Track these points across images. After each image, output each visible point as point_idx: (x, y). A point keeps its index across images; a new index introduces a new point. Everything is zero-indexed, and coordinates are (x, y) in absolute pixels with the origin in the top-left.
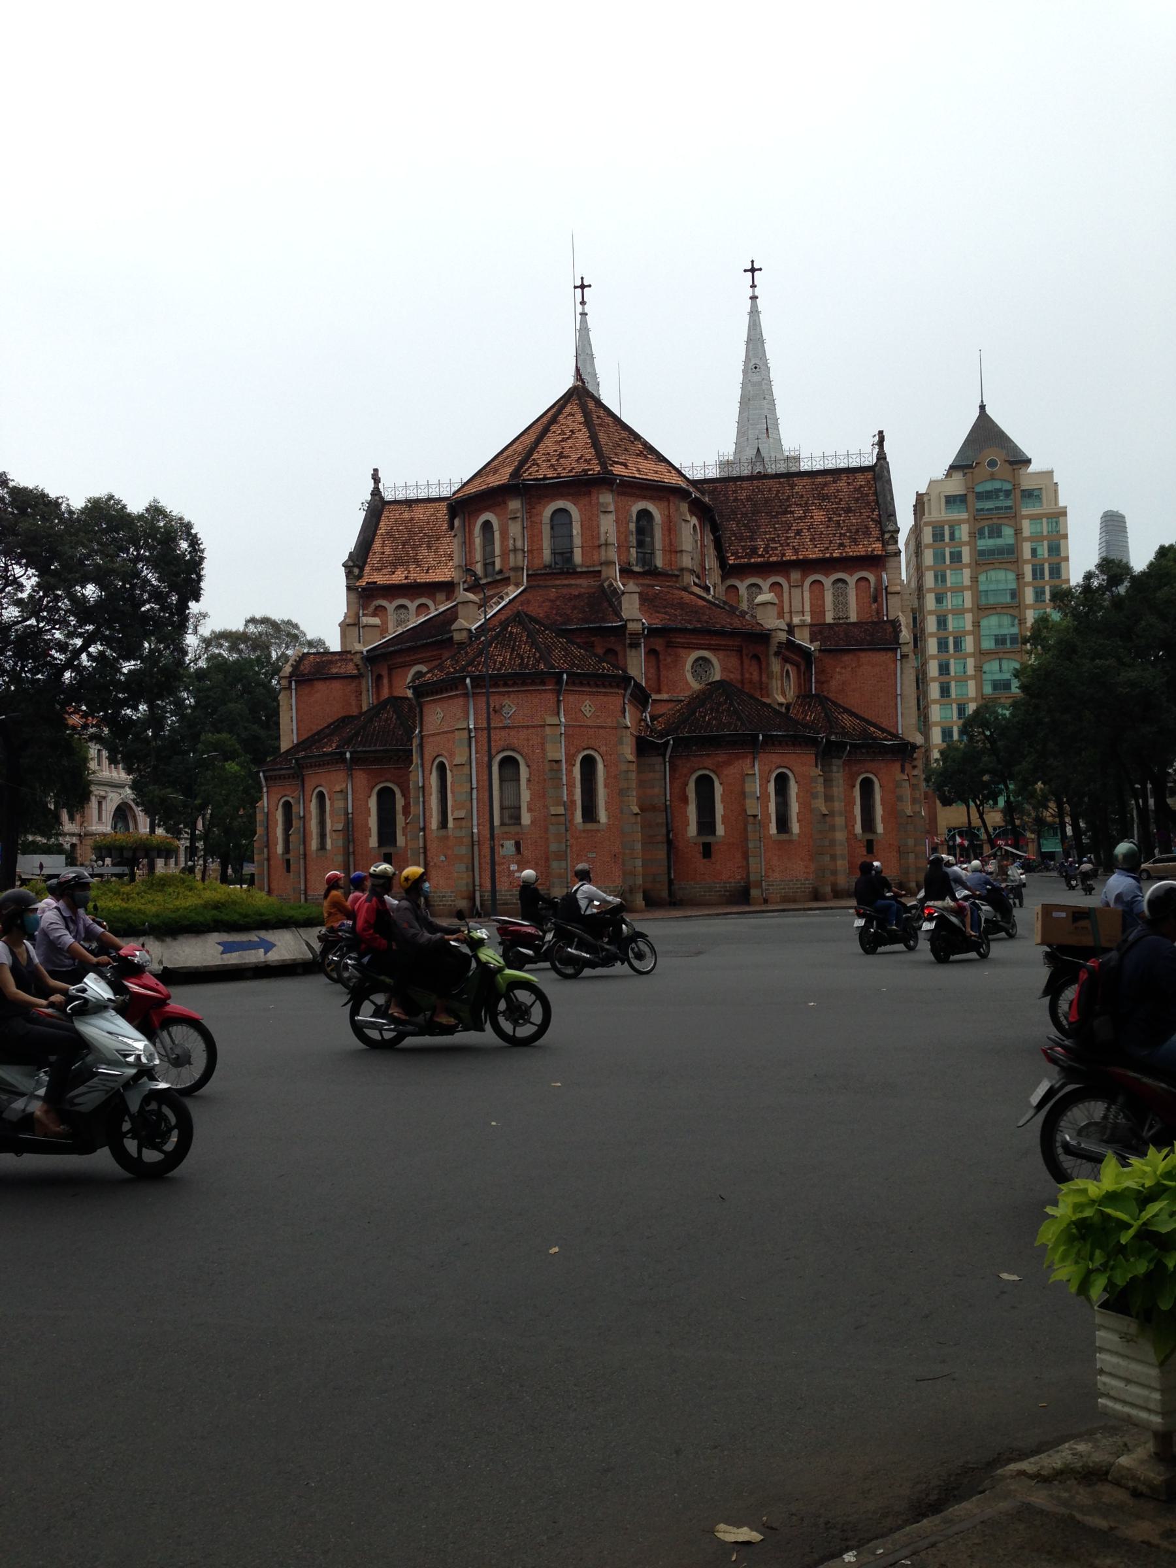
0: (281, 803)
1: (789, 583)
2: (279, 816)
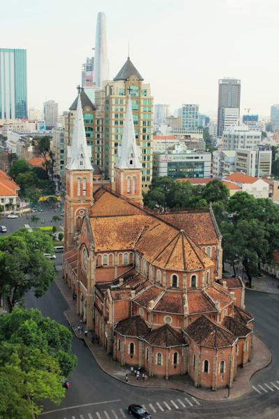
2: (129, 345)
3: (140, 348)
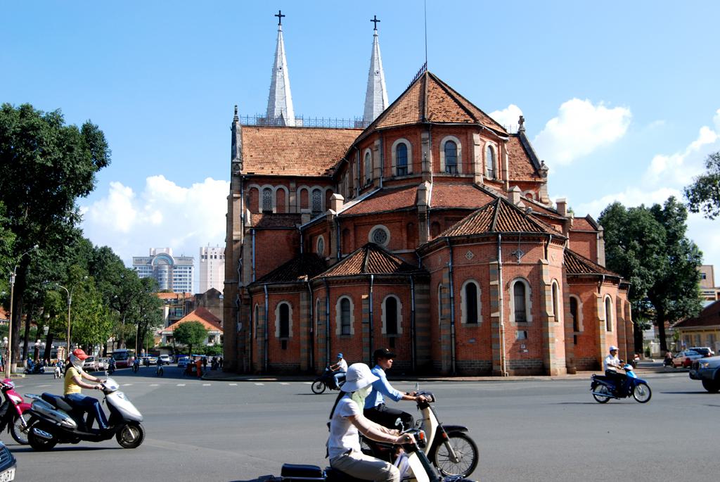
1: (289, 189)
2: (277, 313)
3: (304, 312)
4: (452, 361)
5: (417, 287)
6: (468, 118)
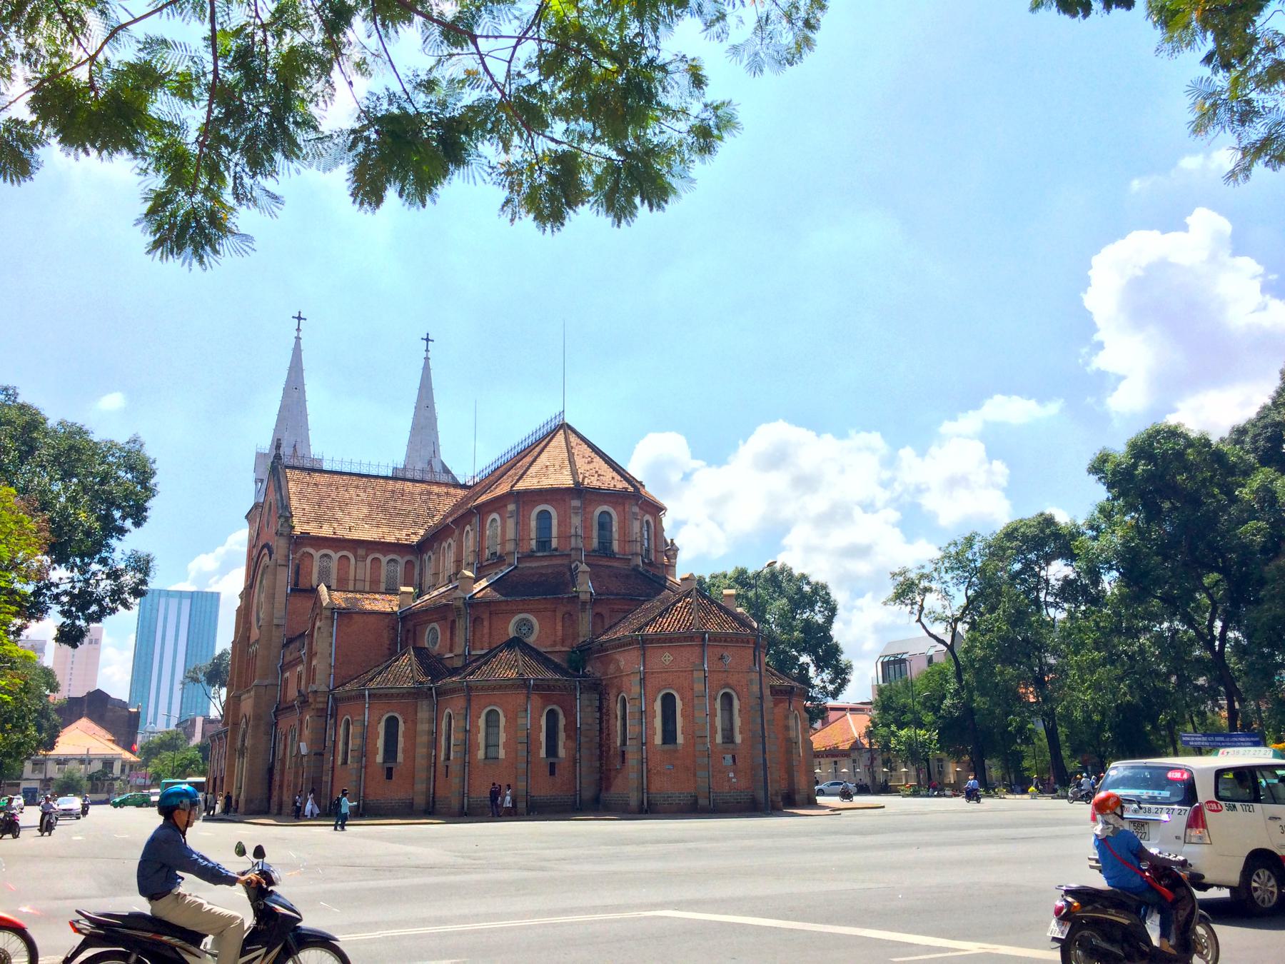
0: (384, 718)
3: (423, 727)
4: (643, 793)
5: (585, 696)
6: (626, 485)
